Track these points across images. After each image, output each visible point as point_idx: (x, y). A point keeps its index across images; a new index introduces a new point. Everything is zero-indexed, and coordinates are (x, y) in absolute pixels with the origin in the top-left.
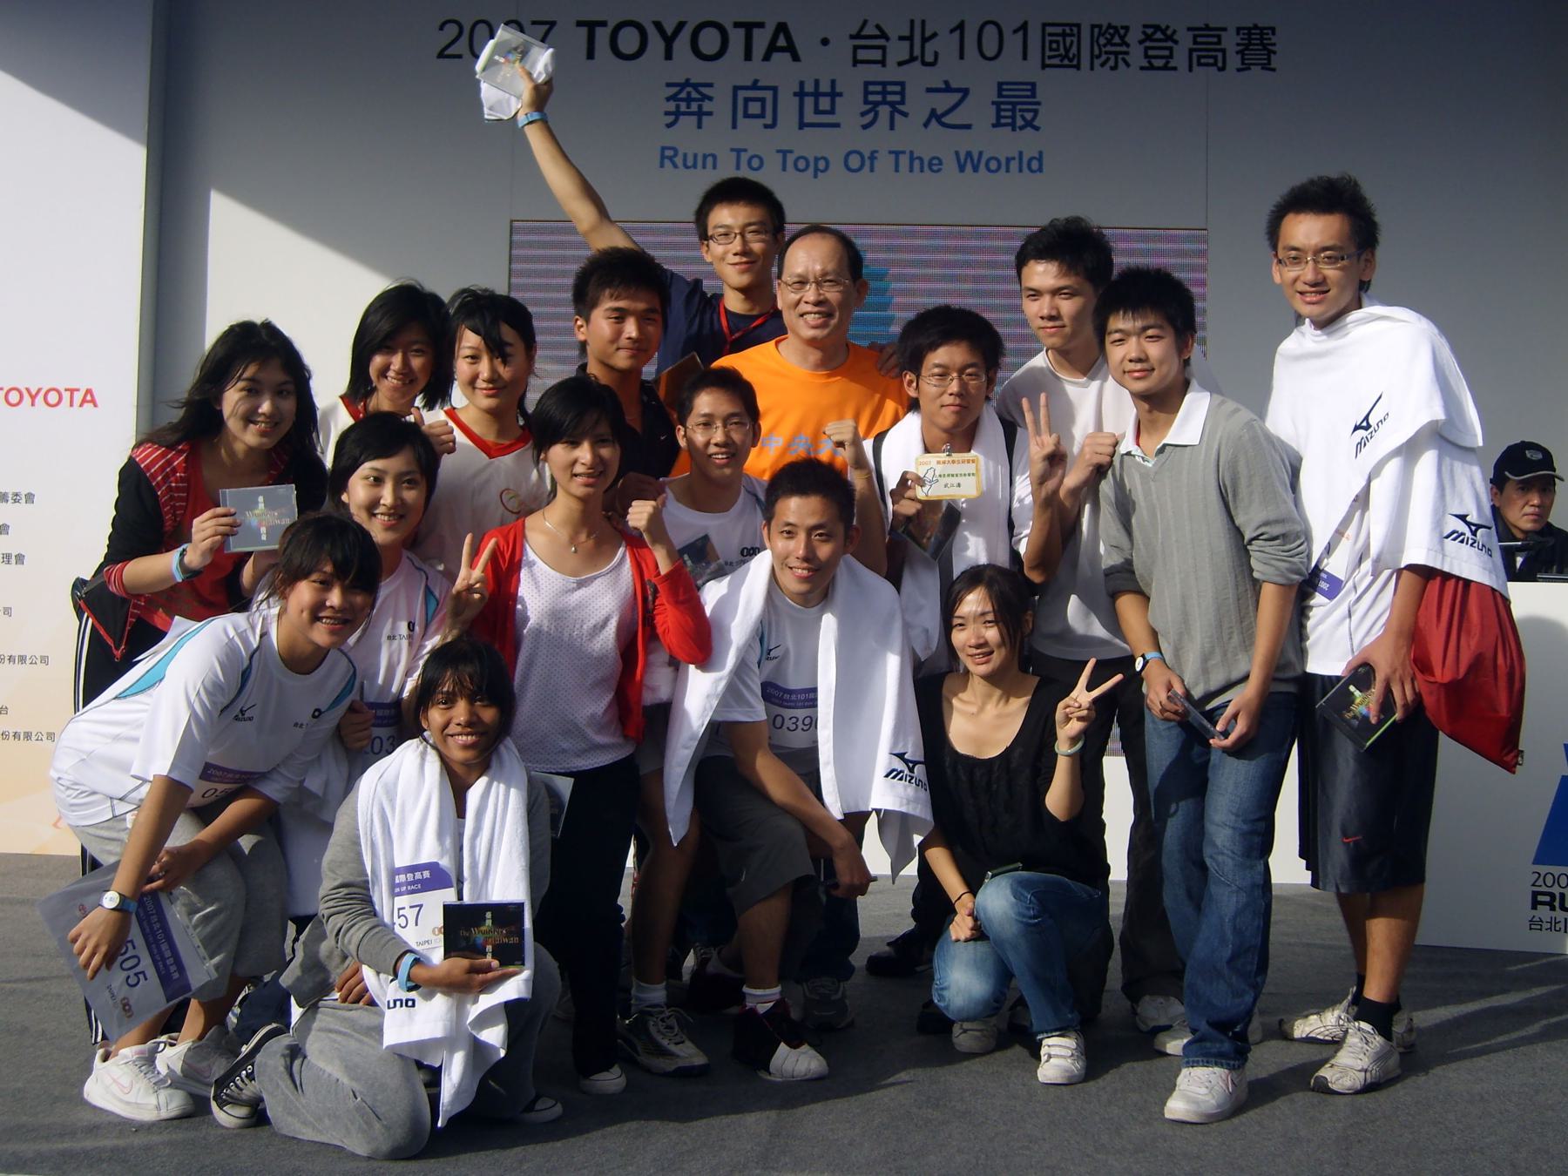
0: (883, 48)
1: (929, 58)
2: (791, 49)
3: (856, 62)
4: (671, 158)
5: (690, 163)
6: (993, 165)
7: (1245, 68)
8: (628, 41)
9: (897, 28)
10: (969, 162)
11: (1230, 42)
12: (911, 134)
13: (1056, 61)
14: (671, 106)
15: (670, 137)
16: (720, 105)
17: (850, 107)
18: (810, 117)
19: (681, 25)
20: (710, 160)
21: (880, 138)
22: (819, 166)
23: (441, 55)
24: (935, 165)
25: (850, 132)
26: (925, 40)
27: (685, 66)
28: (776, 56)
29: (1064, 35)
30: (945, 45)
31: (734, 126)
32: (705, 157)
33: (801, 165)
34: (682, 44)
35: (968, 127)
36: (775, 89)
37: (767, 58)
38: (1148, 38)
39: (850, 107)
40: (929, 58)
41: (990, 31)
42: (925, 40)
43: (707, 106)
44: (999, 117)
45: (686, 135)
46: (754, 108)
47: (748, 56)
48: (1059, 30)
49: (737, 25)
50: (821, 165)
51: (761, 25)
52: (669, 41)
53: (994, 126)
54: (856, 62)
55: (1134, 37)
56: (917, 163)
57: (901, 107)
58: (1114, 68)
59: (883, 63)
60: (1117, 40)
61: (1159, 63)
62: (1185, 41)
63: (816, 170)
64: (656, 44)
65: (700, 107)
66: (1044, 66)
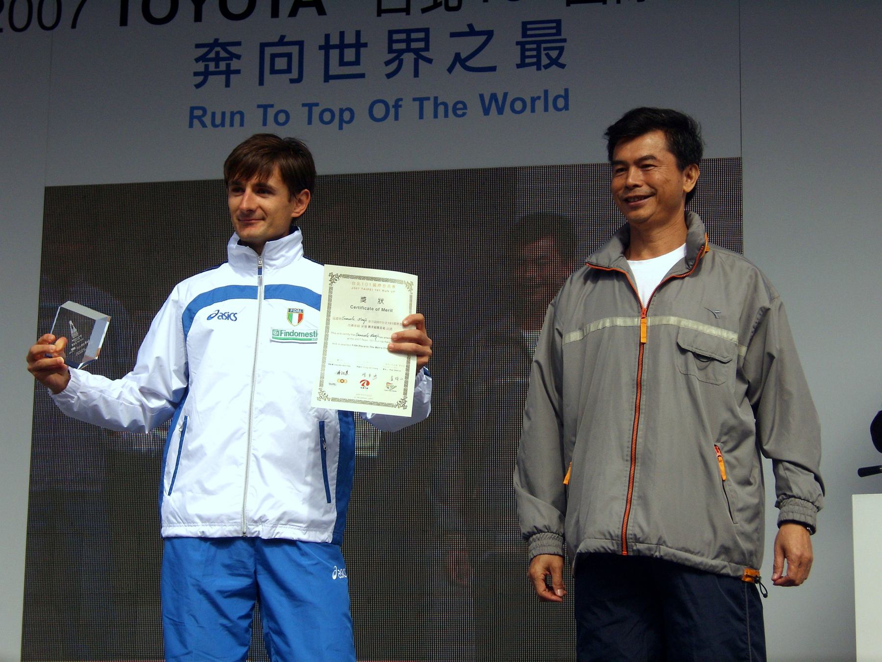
12: (436, 81)
14: (201, 67)
15: (201, 97)
16: (248, 63)
17: (375, 56)
18: (335, 69)
21: (405, 86)
22: (344, 117)
25: (376, 80)
27: (215, 26)
31: (261, 83)
35: (493, 69)
36: (300, 44)
39: (375, 56)
43: (235, 64)
44: (523, 57)
45: (216, 95)
46: (281, 63)
53: (519, 66)
57: (424, 54)
65: (228, 66)
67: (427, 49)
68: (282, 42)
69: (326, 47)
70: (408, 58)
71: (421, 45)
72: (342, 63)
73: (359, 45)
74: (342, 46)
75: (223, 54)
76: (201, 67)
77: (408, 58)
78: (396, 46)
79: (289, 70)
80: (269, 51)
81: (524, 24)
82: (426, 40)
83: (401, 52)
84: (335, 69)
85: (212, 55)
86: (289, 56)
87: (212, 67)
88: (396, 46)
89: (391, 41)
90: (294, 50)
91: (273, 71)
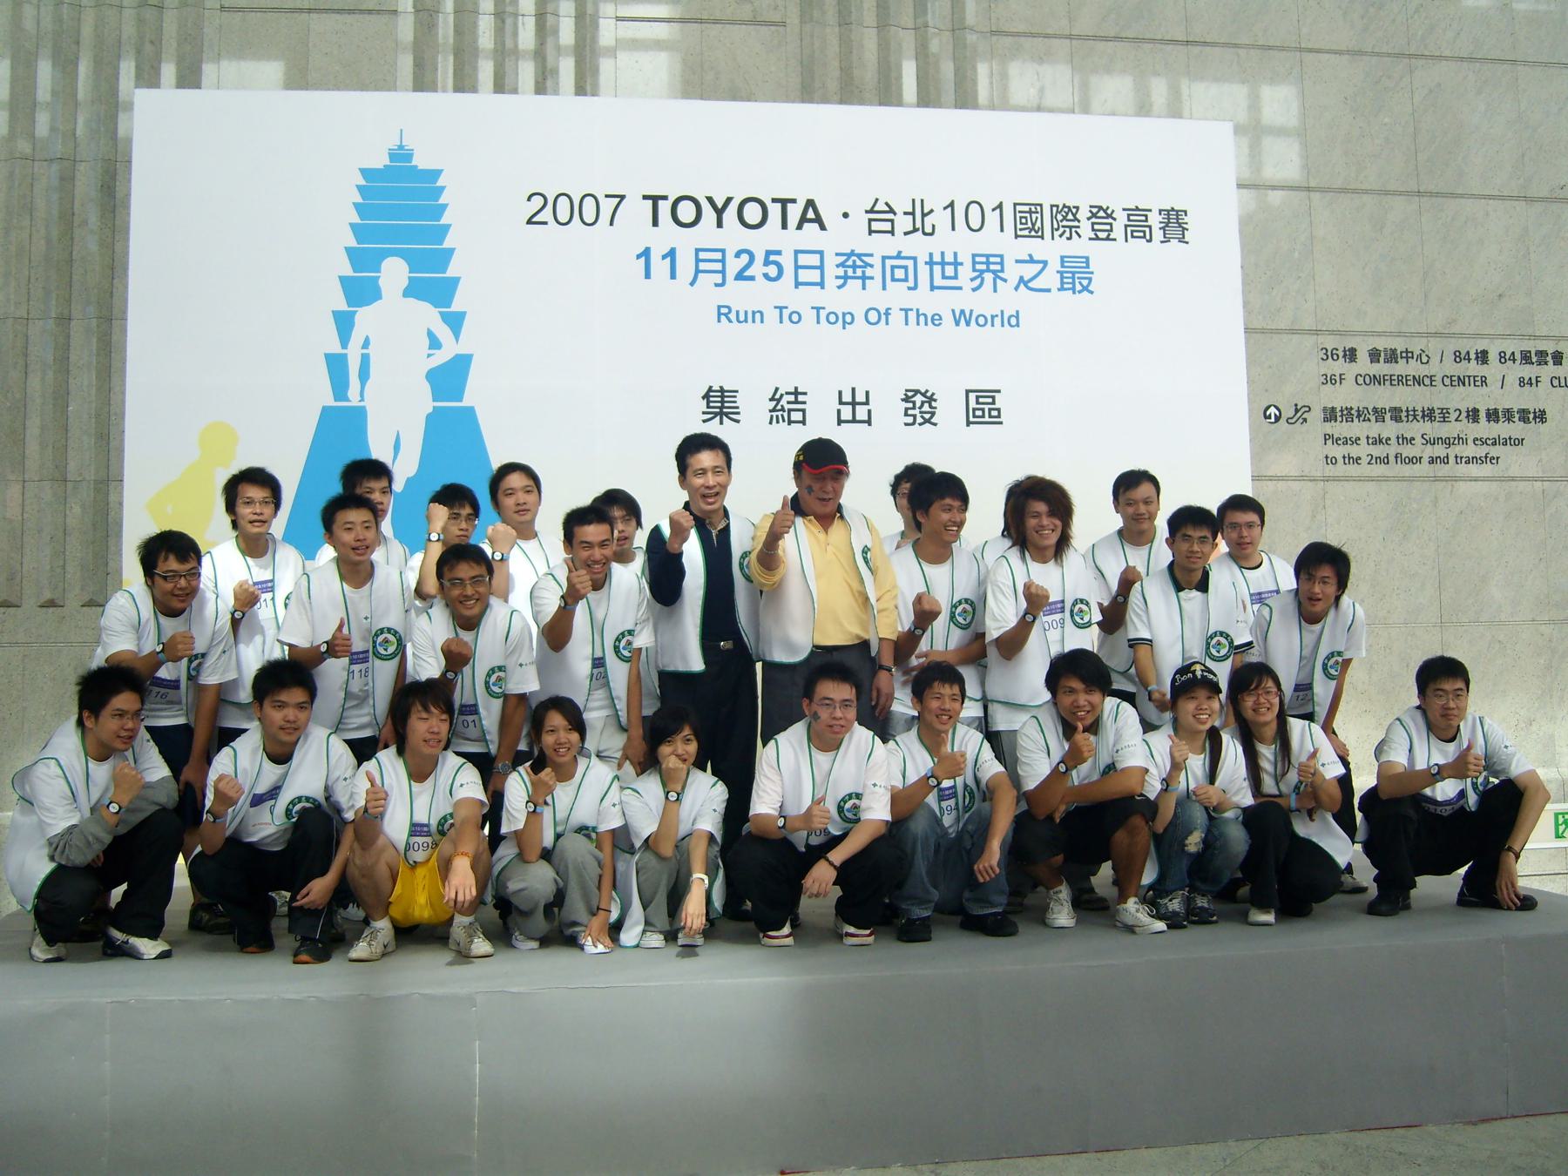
0: (892, 221)
1: (928, 229)
2: (818, 220)
3: (871, 232)
4: (726, 315)
5: (742, 318)
6: (981, 321)
7: (1166, 240)
8: (686, 212)
9: (902, 206)
10: (962, 318)
11: (1155, 220)
13: (1026, 233)
19: (729, 200)
20: (758, 316)
23: (529, 222)
24: (936, 320)
26: (924, 215)
28: (806, 225)
29: (1030, 212)
30: (940, 219)
32: (754, 313)
33: (832, 318)
34: (730, 214)
37: (799, 227)
38: (1094, 215)
40: (928, 229)
41: (974, 207)
42: (924, 215)
47: (784, 226)
48: (1026, 208)
49: (774, 200)
50: (848, 318)
51: (794, 201)
52: (720, 212)
54: (871, 232)
55: (1083, 214)
56: (922, 318)
58: (1069, 238)
59: (892, 232)
60: (1070, 216)
61: (1101, 235)
62: (1121, 219)
63: (844, 322)
64: (709, 214)
66: (1017, 236)
67: (1002, 270)
68: (899, 256)
69: (931, 263)
70: (988, 277)
71: (998, 267)
72: (944, 277)
73: (956, 264)
75: (859, 263)
76: (841, 272)
77: (988, 277)
78: (978, 267)
79: (906, 280)
80: (889, 263)
81: (1062, 258)
82: (1002, 263)
83: (982, 272)
84: (938, 281)
85: (850, 263)
86: (906, 268)
88: (978, 267)
89: (974, 263)
90: (910, 263)
91: (893, 280)
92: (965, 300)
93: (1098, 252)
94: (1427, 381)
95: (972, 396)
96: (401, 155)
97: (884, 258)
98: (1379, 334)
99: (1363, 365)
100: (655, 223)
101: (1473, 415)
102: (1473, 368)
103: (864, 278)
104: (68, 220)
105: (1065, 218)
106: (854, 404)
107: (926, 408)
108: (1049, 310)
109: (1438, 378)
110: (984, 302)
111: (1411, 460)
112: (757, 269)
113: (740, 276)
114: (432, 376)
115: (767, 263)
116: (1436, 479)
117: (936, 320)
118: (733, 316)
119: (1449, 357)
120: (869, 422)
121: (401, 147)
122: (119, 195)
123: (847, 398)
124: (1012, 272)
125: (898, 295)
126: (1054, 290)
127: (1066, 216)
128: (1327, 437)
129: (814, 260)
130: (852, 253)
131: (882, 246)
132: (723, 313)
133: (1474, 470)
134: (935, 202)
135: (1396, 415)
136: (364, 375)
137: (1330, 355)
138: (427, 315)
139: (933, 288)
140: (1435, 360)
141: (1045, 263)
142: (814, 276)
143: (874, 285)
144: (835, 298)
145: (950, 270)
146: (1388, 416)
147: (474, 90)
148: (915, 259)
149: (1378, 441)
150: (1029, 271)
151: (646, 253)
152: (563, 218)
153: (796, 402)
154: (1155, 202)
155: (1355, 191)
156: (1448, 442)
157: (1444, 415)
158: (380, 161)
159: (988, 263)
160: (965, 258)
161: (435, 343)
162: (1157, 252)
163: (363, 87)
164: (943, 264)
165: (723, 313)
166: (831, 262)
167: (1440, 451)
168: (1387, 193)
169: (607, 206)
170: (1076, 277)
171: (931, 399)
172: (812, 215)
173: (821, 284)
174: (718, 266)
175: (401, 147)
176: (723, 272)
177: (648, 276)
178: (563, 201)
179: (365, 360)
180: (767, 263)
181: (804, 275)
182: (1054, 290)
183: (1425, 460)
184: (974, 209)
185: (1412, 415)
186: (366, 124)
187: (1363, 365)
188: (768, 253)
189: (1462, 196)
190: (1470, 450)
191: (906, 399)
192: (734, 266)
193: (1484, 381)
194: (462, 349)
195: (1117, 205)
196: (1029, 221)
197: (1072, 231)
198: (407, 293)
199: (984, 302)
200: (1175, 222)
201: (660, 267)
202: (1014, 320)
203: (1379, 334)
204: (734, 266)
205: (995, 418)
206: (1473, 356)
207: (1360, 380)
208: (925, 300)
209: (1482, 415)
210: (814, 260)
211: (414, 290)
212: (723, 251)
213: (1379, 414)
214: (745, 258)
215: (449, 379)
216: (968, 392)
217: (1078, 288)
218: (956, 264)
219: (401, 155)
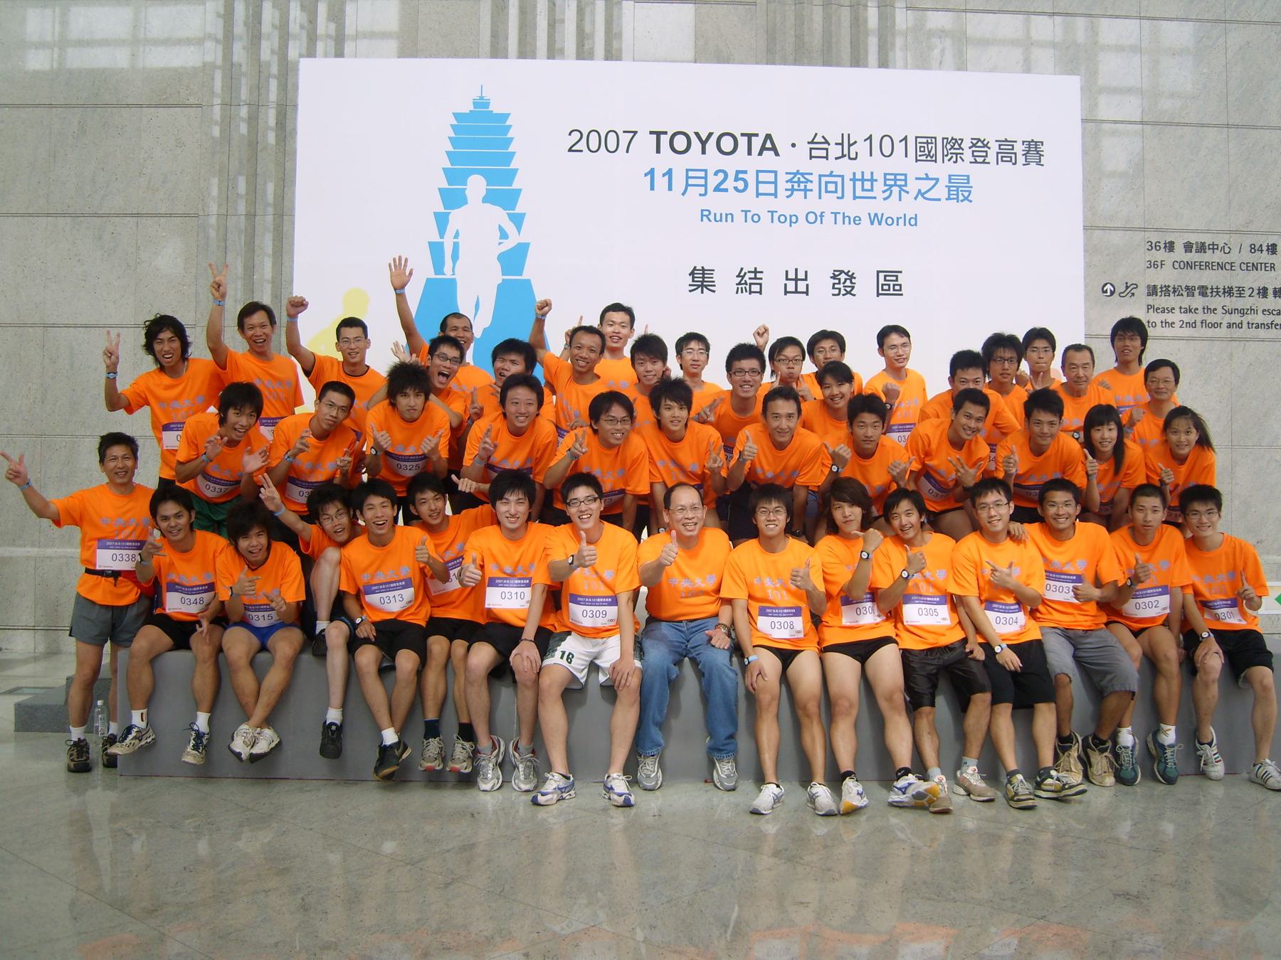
1: (853, 155)
2: (774, 149)
3: (811, 157)
6: (890, 221)
8: (680, 143)
10: (875, 219)
11: (1019, 149)
19: (710, 134)
23: (570, 150)
24: (857, 220)
26: (850, 145)
33: (782, 219)
34: (711, 145)
37: (760, 154)
41: (887, 140)
47: (750, 153)
49: (743, 135)
50: (794, 219)
51: (757, 135)
52: (704, 143)
54: (811, 157)
59: (827, 158)
62: (994, 148)
64: (696, 144)
68: (831, 175)
69: (854, 180)
70: (896, 190)
72: (863, 190)
73: (872, 180)
74: (863, 180)
76: (789, 186)
77: (896, 190)
79: (836, 192)
80: (824, 179)
82: (905, 180)
83: (891, 186)
84: (859, 192)
86: (836, 183)
87: (796, 186)
89: (885, 180)
91: (827, 191)
92: (878, 206)
93: (976, 172)
94: (1228, 267)
95: (882, 275)
96: (481, 103)
97: (820, 176)
98: (1193, 231)
99: (1179, 254)
100: (658, 151)
101: (1263, 292)
102: (1265, 257)
103: (805, 190)
104: (253, 144)
105: (952, 147)
106: (796, 280)
107: (848, 283)
108: (940, 215)
109: (1237, 264)
110: (892, 208)
111: (1213, 325)
112: (730, 184)
113: (717, 189)
114: (502, 258)
115: (736, 179)
116: (1232, 340)
117: (857, 220)
118: (712, 217)
119: (1246, 248)
120: (807, 293)
121: (482, 98)
122: (288, 129)
123: (792, 275)
124: (913, 186)
125: (829, 203)
126: (943, 200)
127: (953, 146)
128: (1149, 307)
129: (771, 177)
130: (795, 174)
131: (818, 167)
132: (705, 214)
133: (1262, 333)
134: (858, 136)
135: (1203, 291)
136: (455, 257)
137: (1154, 246)
138: (498, 215)
139: (855, 197)
140: (1235, 251)
141: (937, 180)
142: (771, 188)
143: (813, 196)
144: (784, 205)
145: (867, 185)
146: (1197, 292)
147: (533, 56)
148: (842, 177)
149: (1189, 310)
150: (925, 185)
151: (651, 173)
152: (593, 147)
153: (755, 278)
154: (1020, 135)
155: (1178, 124)
156: (1242, 312)
157: (1241, 292)
158: (467, 107)
159: (895, 180)
160: (879, 176)
161: (504, 235)
162: (1019, 174)
163: (455, 54)
164: (863, 180)
165: (705, 214)
166: (782, 178)
167: (1236, 318)
168: (1202, 125)
169: (625, 139)
170: (959, 190)
171: (852, 277)
172: (769, 145)
173: (775, 195)
174: (702, 182)
175: (482, 98)
176: (705, 186)
177: (652, 188)
178: (594, 135)
179: (456, 246)
180: (736, 179)
181: (762, 189)
182: (943, 200)
183: (1224, 325)
184: (887, 141)
185: (1216, 292)
186: (459, 81)
187: (1179, 254)
188: (738, 172)
189: (1262, 128)
190: (1260, 318)
191: (834, 277)
192: (713, 181)
193: (1273, 267)
194: (523, 239)
195: (991, 139)
196: (926, 149)
197: (957, 157)
198: (484, 201)
199: (892, 208)
200: (1034, 150)
201: (661, 182)
202: (913, 222)
203: (1193, 231)
204: (713, 181)
205: (898, 291)
206: (1265, 248)
207: (1177, 265)
208: (850, 206)
209: (1270, 292)
210: (771, 177)
211: (489, 198)
212: (706, 171)
213: (1190, 291)
214: (721, 176)
215: (513, 260)
216: (878, 272)
217: (961, 198)
218: (872, 180)
219: (481, 103)
